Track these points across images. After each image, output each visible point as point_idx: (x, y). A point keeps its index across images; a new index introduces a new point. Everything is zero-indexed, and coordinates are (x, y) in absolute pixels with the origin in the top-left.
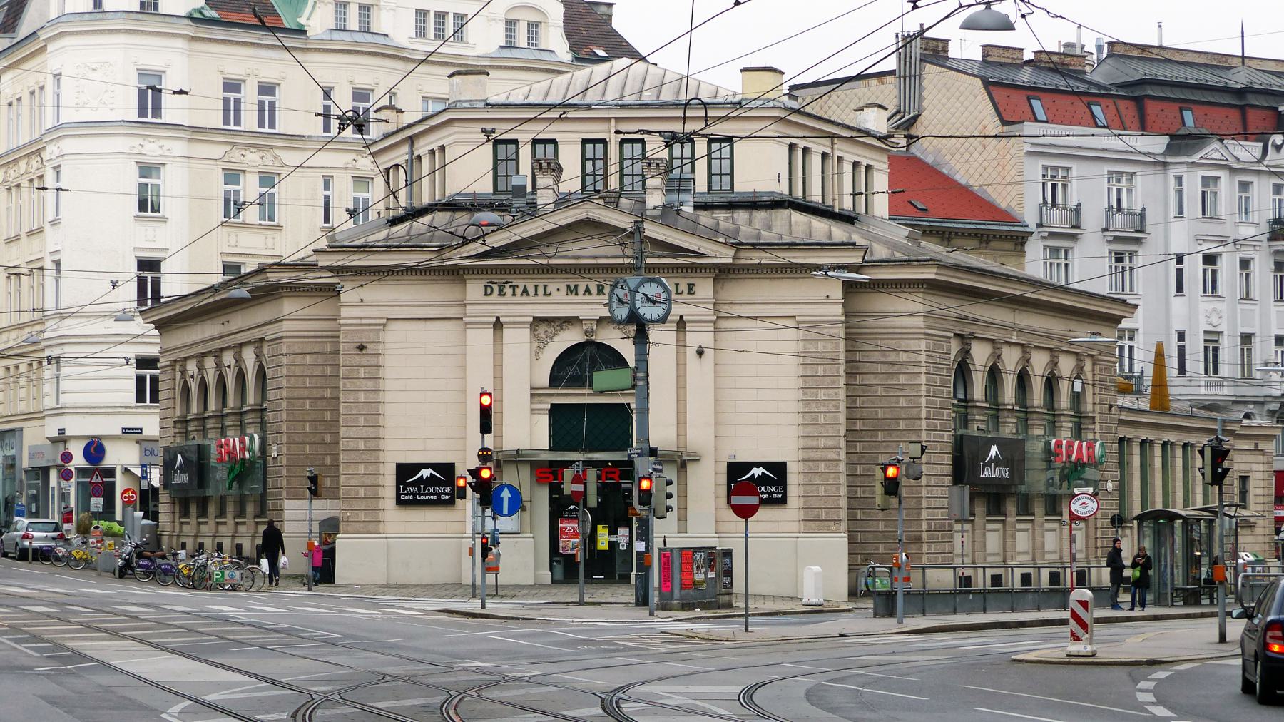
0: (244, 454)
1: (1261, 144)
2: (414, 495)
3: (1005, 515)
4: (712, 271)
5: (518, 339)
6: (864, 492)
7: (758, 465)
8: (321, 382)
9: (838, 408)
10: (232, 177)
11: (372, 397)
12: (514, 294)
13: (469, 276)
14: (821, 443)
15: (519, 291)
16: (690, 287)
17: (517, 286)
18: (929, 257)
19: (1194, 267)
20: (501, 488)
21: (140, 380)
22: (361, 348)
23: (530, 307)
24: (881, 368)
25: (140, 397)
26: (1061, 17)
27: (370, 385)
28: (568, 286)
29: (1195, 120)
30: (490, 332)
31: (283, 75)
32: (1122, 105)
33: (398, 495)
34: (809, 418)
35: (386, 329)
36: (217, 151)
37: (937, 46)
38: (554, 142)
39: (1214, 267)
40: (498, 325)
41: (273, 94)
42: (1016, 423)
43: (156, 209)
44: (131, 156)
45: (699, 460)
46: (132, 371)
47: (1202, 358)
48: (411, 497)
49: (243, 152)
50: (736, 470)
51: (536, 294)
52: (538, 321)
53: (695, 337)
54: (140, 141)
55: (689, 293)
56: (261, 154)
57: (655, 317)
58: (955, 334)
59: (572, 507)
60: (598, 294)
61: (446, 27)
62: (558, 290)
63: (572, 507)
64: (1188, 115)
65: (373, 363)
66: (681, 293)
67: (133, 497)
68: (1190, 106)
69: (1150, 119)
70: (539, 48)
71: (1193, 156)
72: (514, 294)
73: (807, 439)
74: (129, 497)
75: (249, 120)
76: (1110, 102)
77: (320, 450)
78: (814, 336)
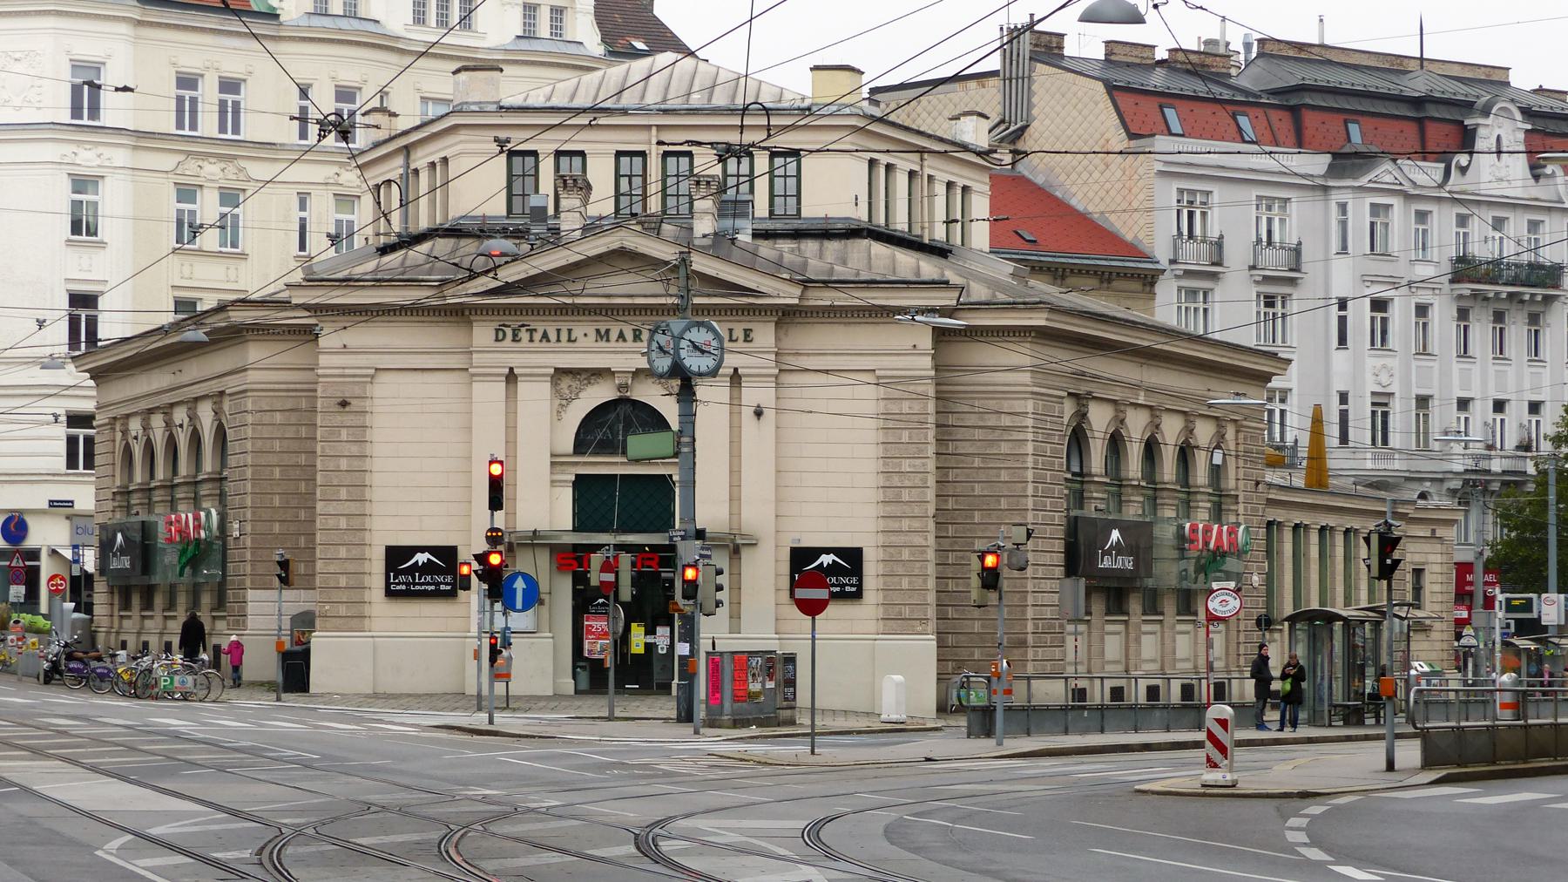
0: (199, 533)
1: (1443, 165)
2: (407, 584)
3: (1127, 614)
4: (774, 313)
5: (535, 396)
6: (957, 585)
7: (827, 551)
8: (294, 446)
9: (926, 483)
10: (186, 193)
11: (356, 464)
12: (531, 340)
13: (478, 318)
15: (538, 336)
16: (747, 332)
17: (535, 330)
18: (1038, 300)
19: (1360, 315)
20: (514, 577)
21: (72, 442)
22: (344, 404)
23: (551, 356)
24: (978, 434)
25: (72, 462)
26: (1201, 8)
27: (354, 449)
28: (598, 331)
29: (1363, 134)
31: (250, 69)
32: (1275, 115)
33: (388, 584)
34: (891, 494)
35: (375, 381)
36: (168, 162)
37: (1050, 42)
38: (582, 154)
39: (1384, 315)
40: (511, 377)
41: (238, 93)
42: (1143, 503)
43: (92, 231)
44: (63, 167)
45: (755, 544)
46: (61, 431)
47: (1369, 426)
48: (404, 587)
49: (200, 163)
50: (801, 557)
51: (558, 340)
52: (561, 372)
53: (753, 394)
54: (73, 148)
55: (745, 341)
56: (223, 165)
57: (704, 369)
58: (1069, 394)
59: (601, 601)
60: (635, 341)
61: (450, 12)
62: (585, 335)
63: (601, 601)
64: (1354, 129)
65: (359, 423)
66: (736, 340)
67: (61, 585)
68: (1355, 117)
69: (1308, 133)
70: (564, 38)
71: (1361, 179)
72: (531, 340)
74: (57, 585)
75: (208, 124)
76: (1259, 112)
77: (293, 528)
78: (897, 394)
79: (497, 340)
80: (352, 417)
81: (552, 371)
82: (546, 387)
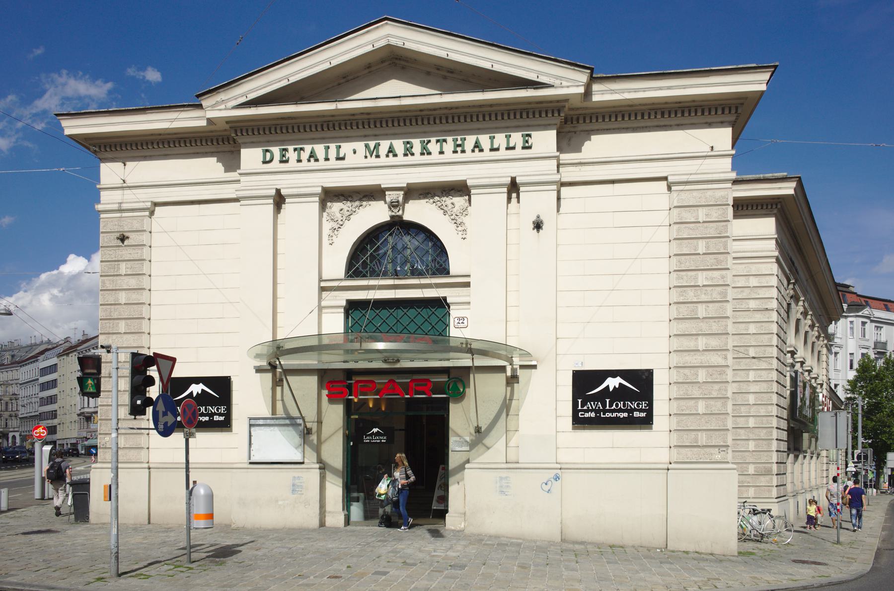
9: (725, 296)
11: (134, 297)
14: (702, 343)
15: (305, 155)
22: (123, 239)
27: (132, 282)
28: (367, 146)
30: (269, 208)
34: (684, 311)
51: (327, 159)
65: (136, 257)
73: (682, 339)
79: (265, 162)
80: (130, 250)
81: (319, 190)
82: (314, 206)
